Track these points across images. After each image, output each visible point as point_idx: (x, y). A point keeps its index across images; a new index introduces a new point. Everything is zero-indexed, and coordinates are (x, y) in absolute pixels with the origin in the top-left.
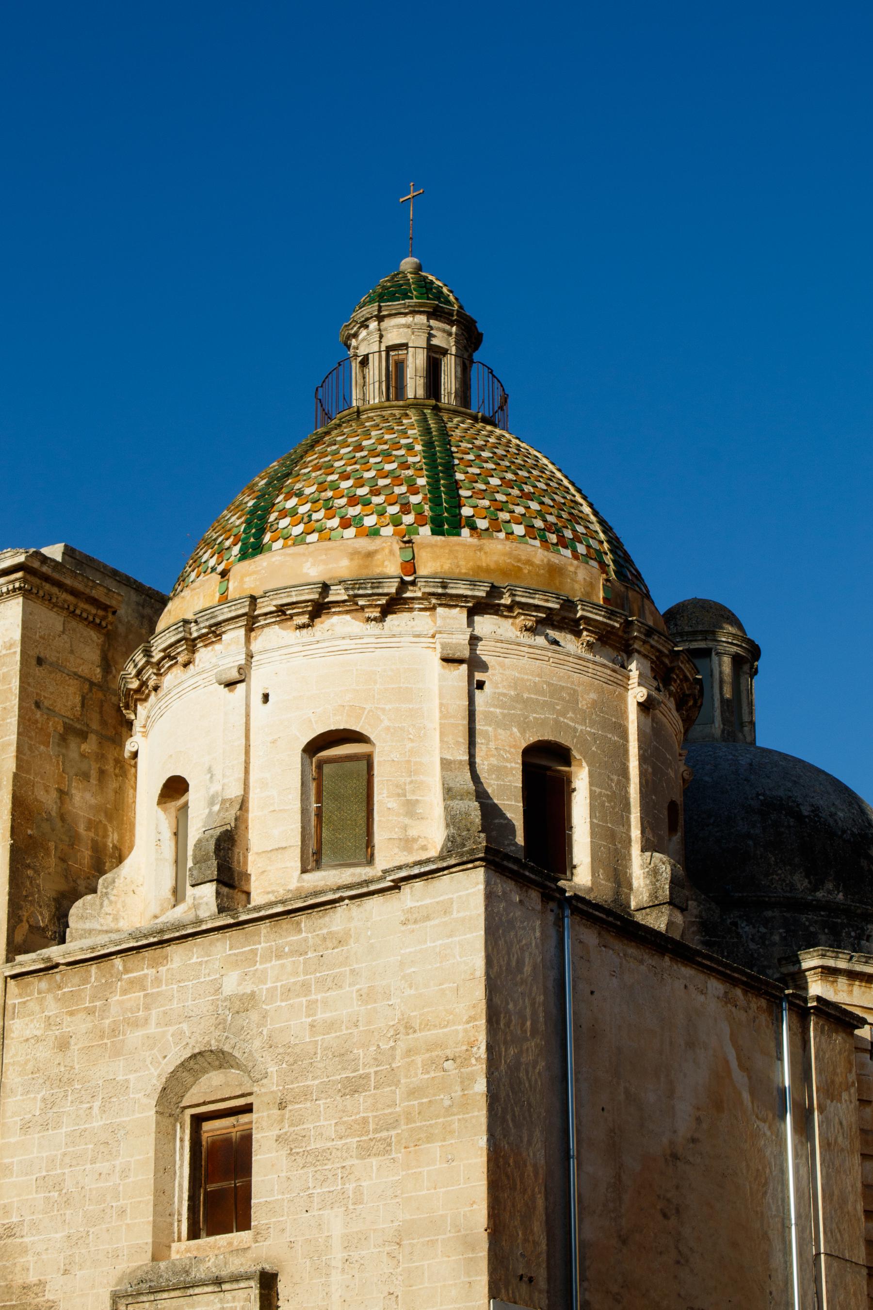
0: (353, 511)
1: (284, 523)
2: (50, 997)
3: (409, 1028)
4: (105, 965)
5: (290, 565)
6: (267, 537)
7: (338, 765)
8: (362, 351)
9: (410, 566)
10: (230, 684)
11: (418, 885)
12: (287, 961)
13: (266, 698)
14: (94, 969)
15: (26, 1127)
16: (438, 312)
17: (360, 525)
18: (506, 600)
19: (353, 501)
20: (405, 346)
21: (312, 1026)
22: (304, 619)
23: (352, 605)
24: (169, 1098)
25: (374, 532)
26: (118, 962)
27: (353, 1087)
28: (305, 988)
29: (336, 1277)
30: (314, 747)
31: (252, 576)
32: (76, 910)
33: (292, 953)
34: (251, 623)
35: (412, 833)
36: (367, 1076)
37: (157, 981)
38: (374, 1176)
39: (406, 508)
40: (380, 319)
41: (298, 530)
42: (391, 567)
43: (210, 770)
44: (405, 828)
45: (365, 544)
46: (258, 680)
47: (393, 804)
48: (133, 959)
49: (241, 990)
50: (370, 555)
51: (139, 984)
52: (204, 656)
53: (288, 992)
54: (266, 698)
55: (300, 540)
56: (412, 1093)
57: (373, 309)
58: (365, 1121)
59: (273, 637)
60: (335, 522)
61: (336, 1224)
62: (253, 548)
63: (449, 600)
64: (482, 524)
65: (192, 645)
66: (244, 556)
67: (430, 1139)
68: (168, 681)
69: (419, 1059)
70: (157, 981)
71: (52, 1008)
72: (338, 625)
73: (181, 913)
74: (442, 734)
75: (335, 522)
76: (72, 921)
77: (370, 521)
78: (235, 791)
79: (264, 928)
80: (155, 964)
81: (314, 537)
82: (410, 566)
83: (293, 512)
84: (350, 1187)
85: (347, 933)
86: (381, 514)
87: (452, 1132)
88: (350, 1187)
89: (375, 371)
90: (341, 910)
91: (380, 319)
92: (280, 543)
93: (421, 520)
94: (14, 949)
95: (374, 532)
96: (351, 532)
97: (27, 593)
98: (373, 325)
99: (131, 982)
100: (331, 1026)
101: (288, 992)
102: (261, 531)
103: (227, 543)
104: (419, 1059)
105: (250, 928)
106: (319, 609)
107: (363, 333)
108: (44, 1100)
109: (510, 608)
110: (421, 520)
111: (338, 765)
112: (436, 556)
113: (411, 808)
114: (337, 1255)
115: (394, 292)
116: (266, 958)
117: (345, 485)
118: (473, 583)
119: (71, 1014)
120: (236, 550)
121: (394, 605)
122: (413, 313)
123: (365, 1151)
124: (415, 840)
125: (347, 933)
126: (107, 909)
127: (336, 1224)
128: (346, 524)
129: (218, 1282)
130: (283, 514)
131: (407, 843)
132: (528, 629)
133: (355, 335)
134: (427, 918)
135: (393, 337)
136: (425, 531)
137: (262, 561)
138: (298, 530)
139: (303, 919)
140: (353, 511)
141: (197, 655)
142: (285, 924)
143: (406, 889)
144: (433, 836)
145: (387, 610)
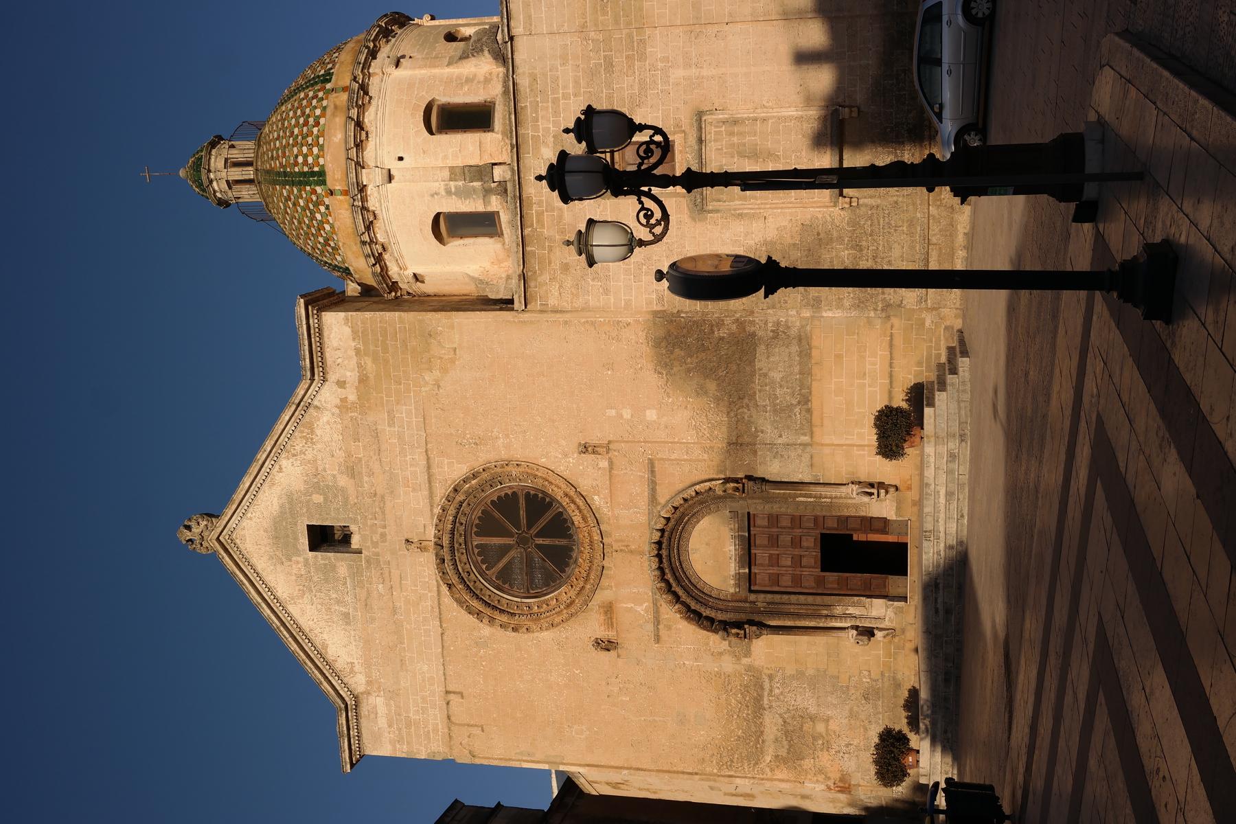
0: (311, 120)
1: (310, 160)
2: (539, 279)
3: (584, 26)
4: (527, 240)
5: (333, 158)
6: (316, 169)
8: (224, 186)
9: (345, 89)
10: (390, 178)
11: (512, 24)
13: (401, 159)
14: (528, 249)
15: (606, 292)
16: (213, 145)
17: (319, 117)
18: (371, 45)
19: (306, 123)
20: (226, 160)
21: (575, 95)
22: (364, 133)
23: (362, 108)
25: (325, 108)
26: (526, 232)
27: (609, 65)
28: (556, 101)
29: (705, 72)
30: (431, 133)
31: (336, 178)
33: (536, 112)
34: (360, 165)
35: (482, 79)
36: (605, 57)
37: (540, 203)
38: (656, 49)
39: (315, 97)
40: (209, 171)
41: (315, 150)
42: (344, 97)
43: (432, 196)
45: (329, 112)
48: (527, 222)
49: (551, 145)
50: (336, 107)
51: (540, 214)
52: (372, 204)
53: (556, 113)
54: (401, 159)
55: (321, 148)
56: (617, 22)
57: (204, 172)
58: (627, 57)
59: (369, 154)
60: (315, 130)
61: (678, 74)
62: (320, 177)
63: (366, 65)
64: (330, 66)
65: (364, 208)
66: (323, 183)
67: (641, 9)
68: (381, 237)
69: (601, 18)
70: (540, 203)
71: (545, 277)
72: (369, 118)
75: (315, 130)
77: (318, 112)
78: (447, 174)
79: (521, 131)
80: (530, 205)
81: (321, 140)
82: (345, 89)
83: (305, 157)
84: (660, 65)
85: (531, 75)
86: (315, 107)
88: (660, 65)
89: (236, 174)
90: (518, 80)
91: (209, 171)
92: (321, 161)
93: (323, 89)
96: (322, 121)
97: (320, 310)
98: (212, 176)
99: (538, 222)
100: (577, 82)
101: (556, 113)
102: (313, 174)
103: (314, 198)
104: (601, 18)
105: (520, 140)
106: (359, 125)
107: (215, 184)
108: (593, 280)
109: (375, 46)
110: (323, 89)
112: (342, 76)
113: (469, 80)
114: (693, 71)
115: (197, 166)
116: (536, 128)
117: (296, 131)
118: (360, 52)
119: (550, 263)
120: (319, 189)
121: (364, 88)
122: (210, 154)
123: (642, 57)
124: (486, 78)
125: (531, 75)
127: (678, 74)
128: (317, 124)
129: (700, 141)
130: (305, 162)
131: (487, 80)
132: (388, 42)
133: (215, 192)
134: (530, 17)
135: (221, 164)
136: (329, 86)
137: (329, 169)
138: (315, 150)
139: (520, 105)
140: (311, 120)
141: (371, 208)
142: (521, 117)
143: (514, 32)
144: (484, 66)
145: (366, 93)
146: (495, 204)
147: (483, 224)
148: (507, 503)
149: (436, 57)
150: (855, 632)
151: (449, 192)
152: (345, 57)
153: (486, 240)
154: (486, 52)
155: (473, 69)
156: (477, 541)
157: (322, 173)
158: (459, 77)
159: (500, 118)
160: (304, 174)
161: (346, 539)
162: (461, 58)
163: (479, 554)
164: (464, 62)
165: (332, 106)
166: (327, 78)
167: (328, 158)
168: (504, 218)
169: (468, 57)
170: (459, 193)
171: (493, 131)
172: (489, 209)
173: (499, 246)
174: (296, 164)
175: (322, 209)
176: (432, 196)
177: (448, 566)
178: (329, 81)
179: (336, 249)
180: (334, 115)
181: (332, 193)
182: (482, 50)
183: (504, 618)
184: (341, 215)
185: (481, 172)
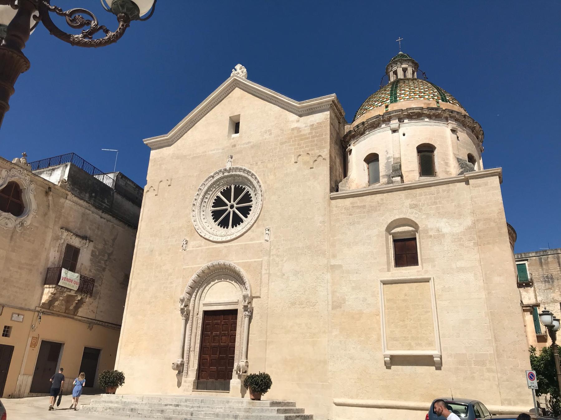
6: (398, 99)
7: (426, 153)
12: (428, 197)
13: (404, 135)
19: (421, 92)
24: (389, 229)
25: (428, 99)
32: (340, 185)
35: (448, 170)
43: (386, 151)
44: (446, 168)
45: (427, 101)
46: (401, 131)
47: (442, 162)
50: (429, 104)
54: (404, 135)
66: (391, 102)
73: (376, 186)
74: (453, 147)
76: (340, 187)
77: (427, 97)
78: (397, 156)
87: (496, 242)
94: (331, 191)
95: (428, 99)
96: (422, 99)
111: (426, 153)
113: (447, 164)
126: (347, 185)
130: (401, 94)
131: (447, 172)
134: (480, 186)
136: (440, 101)
138: (408, 97)
146: (383, 180)
147: (374, 178)
148: (247, 198)
149: (458, 149)
150: (179, 363)
151: (388, 158)
152: (456, 108)
153: (367, 180)
154: (461, 170)
155: (452, 166)
156: (233, 187)
157: (396, 101)
158: (448, 159)
159: (427, 179)
160: (396, 94)
161: (237, 131)
162: (458, 159)
163: (227, 188)
164: (456, 161)
165: (429, 102)
166: (444, 100)
167: (403, 103)
168: (376, 186)
169: (458, 162)
170: (388, 163)
171: (421, 176)
172: (381, 178)
173: (364, 185)
174: (400, 90)
175: (380, 104)
176: (386, 151)
177: (221, 175)
178: (443, 101)
179: (363, 114)
180: (425, 104)
181: (387, 107)
182: (462, 168)
183: (199, 200)
184: (377, 111)
185: (397, 170)
